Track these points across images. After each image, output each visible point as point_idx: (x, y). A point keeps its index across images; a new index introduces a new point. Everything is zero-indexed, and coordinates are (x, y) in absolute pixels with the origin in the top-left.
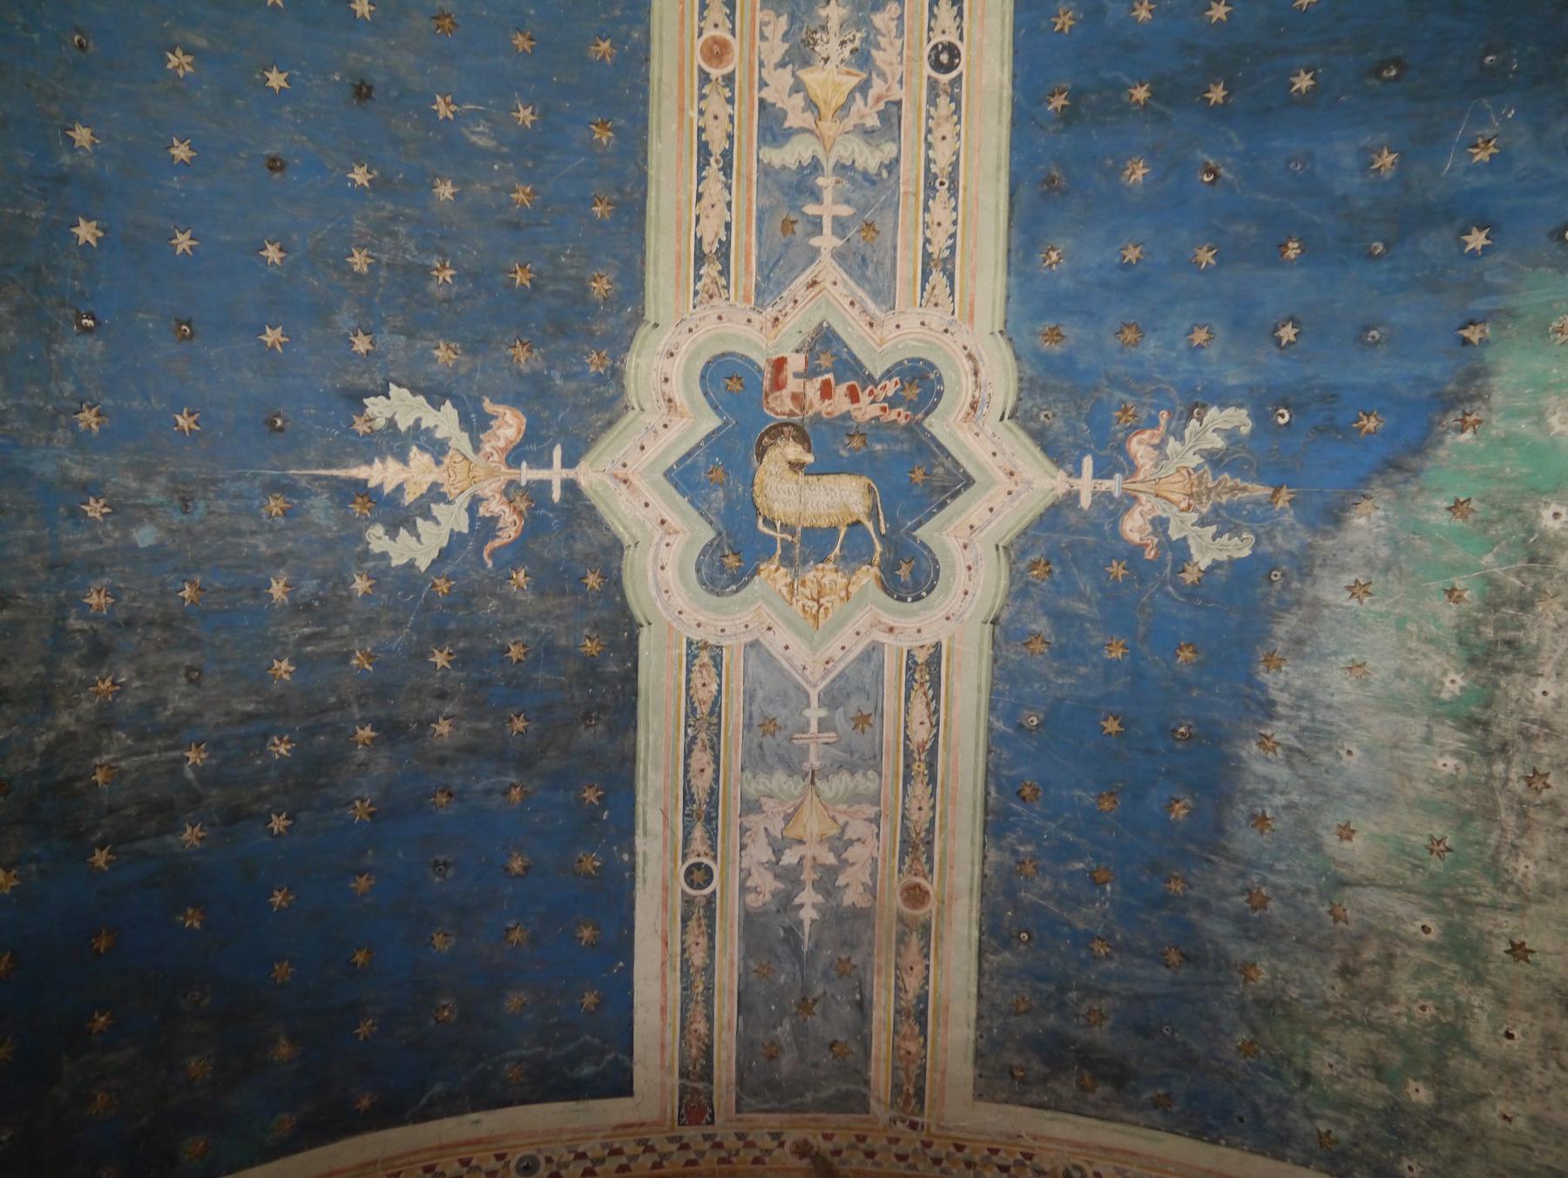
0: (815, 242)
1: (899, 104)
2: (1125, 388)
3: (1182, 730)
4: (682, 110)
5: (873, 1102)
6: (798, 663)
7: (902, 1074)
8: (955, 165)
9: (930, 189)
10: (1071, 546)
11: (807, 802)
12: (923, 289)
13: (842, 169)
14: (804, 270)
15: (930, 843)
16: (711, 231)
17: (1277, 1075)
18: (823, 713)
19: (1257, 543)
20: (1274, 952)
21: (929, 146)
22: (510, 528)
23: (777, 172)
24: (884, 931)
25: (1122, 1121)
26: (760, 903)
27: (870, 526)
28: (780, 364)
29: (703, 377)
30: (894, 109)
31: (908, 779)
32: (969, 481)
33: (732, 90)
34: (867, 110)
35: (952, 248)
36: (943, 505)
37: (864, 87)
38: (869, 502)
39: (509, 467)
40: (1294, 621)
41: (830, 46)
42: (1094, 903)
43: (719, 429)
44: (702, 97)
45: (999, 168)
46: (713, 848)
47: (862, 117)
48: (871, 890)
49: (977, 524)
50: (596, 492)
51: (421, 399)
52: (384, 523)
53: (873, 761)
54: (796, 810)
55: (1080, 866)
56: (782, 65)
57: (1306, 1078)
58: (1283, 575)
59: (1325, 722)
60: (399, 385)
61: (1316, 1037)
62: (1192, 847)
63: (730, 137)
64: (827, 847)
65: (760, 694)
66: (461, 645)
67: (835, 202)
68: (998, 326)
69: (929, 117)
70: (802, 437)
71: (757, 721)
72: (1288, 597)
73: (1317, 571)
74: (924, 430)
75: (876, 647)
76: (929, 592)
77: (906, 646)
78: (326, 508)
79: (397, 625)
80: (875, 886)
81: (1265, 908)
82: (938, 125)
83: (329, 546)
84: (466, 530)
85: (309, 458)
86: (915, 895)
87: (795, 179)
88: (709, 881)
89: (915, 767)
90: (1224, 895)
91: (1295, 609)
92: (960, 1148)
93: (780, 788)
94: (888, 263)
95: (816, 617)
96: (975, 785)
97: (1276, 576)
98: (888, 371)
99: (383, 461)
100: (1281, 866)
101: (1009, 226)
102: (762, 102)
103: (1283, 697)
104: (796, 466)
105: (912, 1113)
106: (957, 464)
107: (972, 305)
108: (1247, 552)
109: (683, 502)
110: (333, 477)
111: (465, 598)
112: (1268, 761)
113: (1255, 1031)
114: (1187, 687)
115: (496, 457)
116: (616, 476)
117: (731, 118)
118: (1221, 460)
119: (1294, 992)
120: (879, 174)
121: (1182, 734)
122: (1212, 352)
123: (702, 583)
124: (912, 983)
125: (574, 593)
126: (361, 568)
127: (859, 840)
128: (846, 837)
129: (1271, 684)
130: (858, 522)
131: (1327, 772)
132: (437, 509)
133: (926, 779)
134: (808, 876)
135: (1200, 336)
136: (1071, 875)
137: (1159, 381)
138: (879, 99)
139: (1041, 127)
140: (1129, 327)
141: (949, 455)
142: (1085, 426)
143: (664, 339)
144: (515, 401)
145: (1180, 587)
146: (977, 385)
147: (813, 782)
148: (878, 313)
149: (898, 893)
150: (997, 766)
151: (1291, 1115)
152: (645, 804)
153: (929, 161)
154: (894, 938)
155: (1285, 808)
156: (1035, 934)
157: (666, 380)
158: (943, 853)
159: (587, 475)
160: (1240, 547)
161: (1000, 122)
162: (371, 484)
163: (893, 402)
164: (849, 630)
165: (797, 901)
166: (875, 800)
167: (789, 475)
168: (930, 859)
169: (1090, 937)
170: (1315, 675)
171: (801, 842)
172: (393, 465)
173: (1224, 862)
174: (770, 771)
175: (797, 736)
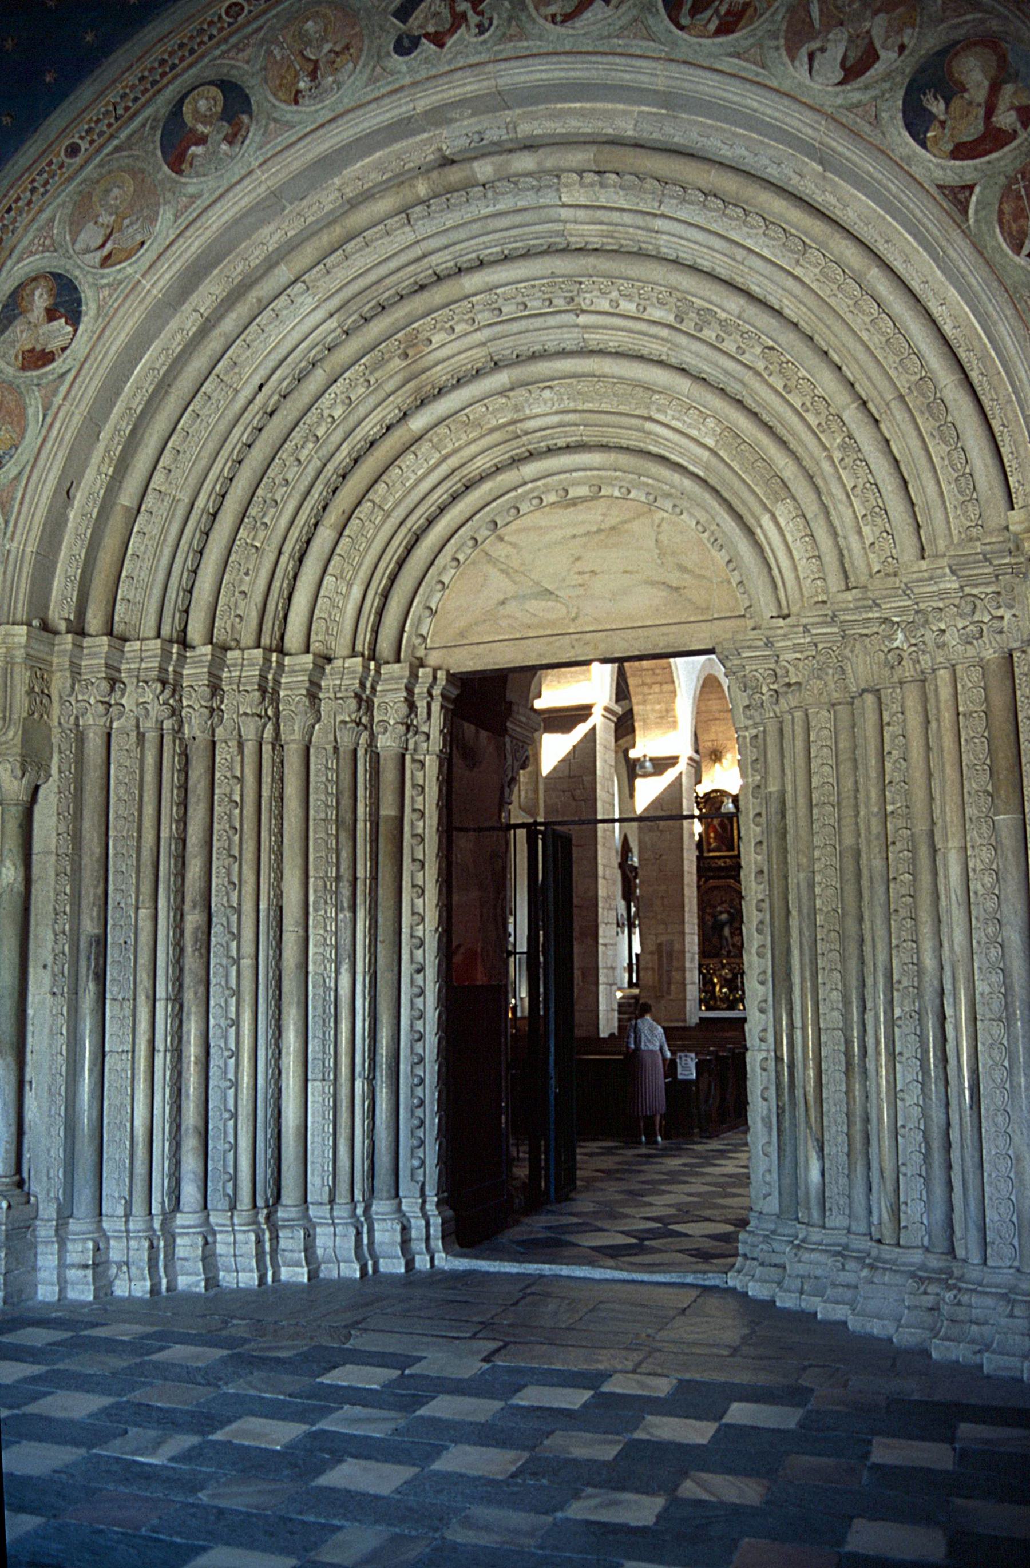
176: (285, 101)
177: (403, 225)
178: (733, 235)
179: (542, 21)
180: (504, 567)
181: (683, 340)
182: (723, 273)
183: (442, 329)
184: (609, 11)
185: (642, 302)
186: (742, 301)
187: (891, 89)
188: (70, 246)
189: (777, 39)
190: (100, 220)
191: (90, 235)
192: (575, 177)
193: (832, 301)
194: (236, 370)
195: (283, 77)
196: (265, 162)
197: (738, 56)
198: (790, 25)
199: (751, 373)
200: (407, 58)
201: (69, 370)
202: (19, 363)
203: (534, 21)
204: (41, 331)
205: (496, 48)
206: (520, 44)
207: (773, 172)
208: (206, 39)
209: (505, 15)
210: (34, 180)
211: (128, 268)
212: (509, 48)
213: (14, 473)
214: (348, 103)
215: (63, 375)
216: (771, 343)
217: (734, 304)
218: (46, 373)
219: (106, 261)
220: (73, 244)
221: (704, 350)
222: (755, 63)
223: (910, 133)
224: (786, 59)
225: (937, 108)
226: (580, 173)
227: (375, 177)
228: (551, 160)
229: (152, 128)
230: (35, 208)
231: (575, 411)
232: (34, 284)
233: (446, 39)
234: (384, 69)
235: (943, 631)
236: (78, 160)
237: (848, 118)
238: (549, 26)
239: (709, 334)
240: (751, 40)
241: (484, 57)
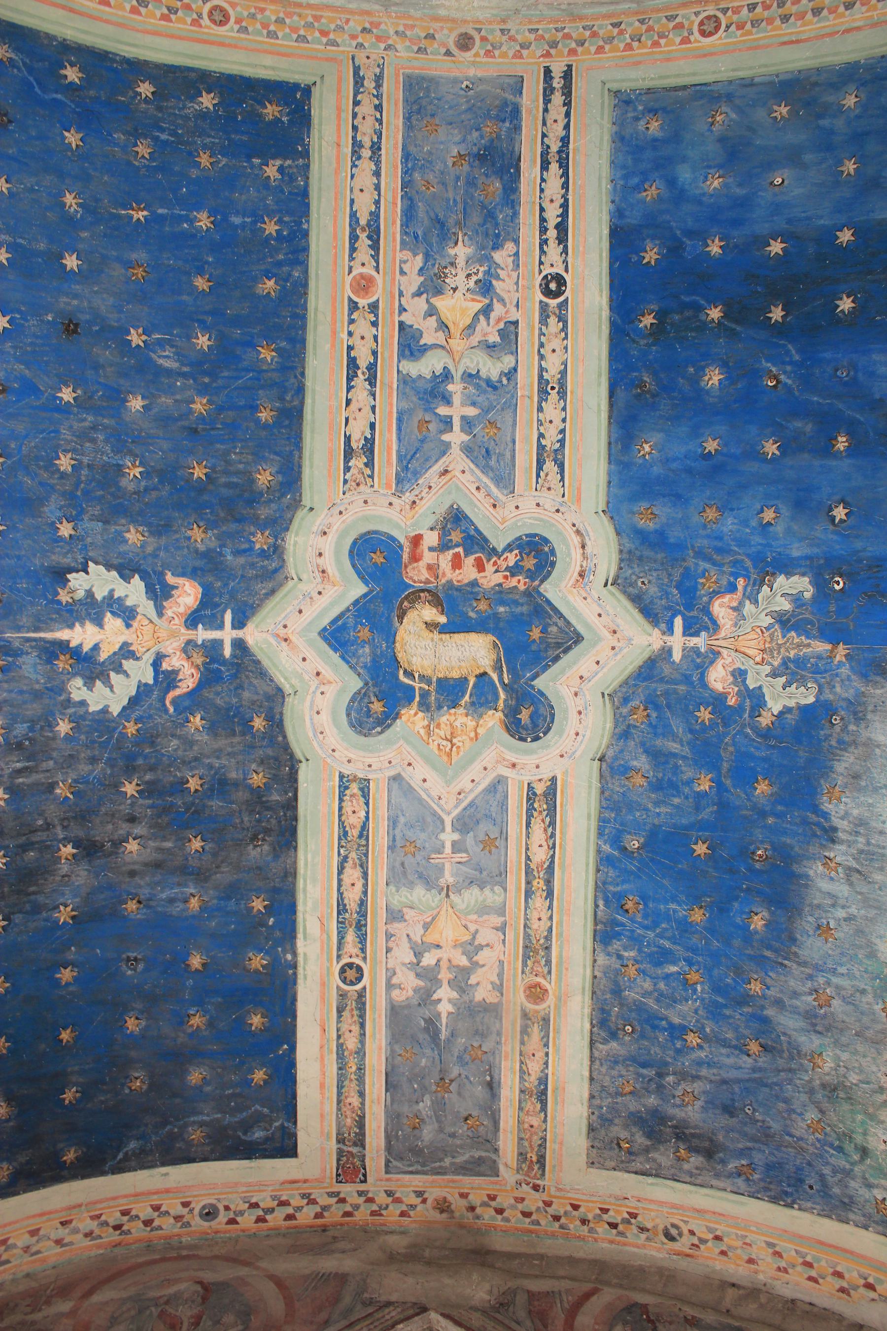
0: (446, 437)
1: (516, 323)
2: (708, 559)
3: (760, 852)
4: (334, 333)
5: (502, 1168)
6: (435, 794)
7: (526, 1144)
8: (563, 373)
9: (543, 393)
10: (666, 693)
11: (443, 912)
12: (538, 476)
13: (470, 377)
14: (436, 461)
15: (548, 948)
16: (358, 431)
17: (840, 1149)
18: (456, 836)
19: (820, 691)
20: (836, 1043)
21: (542, 357)
22: (189, 679)
23: (414, 381)
24: (511, 1023)
25: (712, 1187)
26: (404, 998)
27: (495, 677)
28: (416, 540)
29: (351, 552)
30: (512, 328)
31: (529, 894)
32: (578, 638)
33: (377, 316)
34: (489, 329)
35: (562, 442)
36: (556, 659)
37: (486, 311)
38: (494, 657)
39: (187, 628)
40: (852, 759)
41: (458, 278)
42: (687, 1001)
43: (365, 596)
44: (352, 322)
45: (600, 375)
46: (363, 950)
47: (485, 335)
48: (499, 988)
49: (585, 676)
50: (261, 649)
51: (114, 573)
52: (83, 677)
53: (500, 877)
54: (433, 919)
55: (674, 969)
56: (418, 294)
57: (864, 1152)
58: (842, 719)
59: (878, 846)
60: (96, 563)
61: (872, 1117)
62: (768, 953)
63: (375, 353)
64: (460, 950)
65: (402, 820)
66: (148, 777)
67: (463, 405)
68: (602, 506)
69: (542, 334)
70: (436, 601)
71: (399, 843)
72: (846, 739)
73: (869, 716)
74: (540, 595)
75: (500, 782)
76: (545, 734)
77: (526, 779)
78: (35, 665)
79: (93, 760)
80: (502, 985)
81: (830, 1006)
82: (549, 341)
83: (37, 695)
84: (151, 682)
85: (21, 624)
86: (536, 993)
87: (429, 386)
88: (359, 979)
89: (535, 883)
90: (795, 994)
91: (851, 749)
92: (576, 1207)
93: (420, 900)
94: (508, 455)
95: (449, 755)
96: (586, 899)
97: (836, 719)
98: (509, 545)
99: (82, 625)
100: (842, 970)
101: (610, 423)
102: (401, 324)
103: (842, 824)
104: (431, 626)
105: (535, 1177)
106: (568, 623)
107: (579, 489)
108: (811, 700)
109: (335, 657)
110: (41, 639)
111: (149, 738)
112: (832, 879)
113: (822, 1112)
114: (763, 814)
115: (177, 621)
116: (278, 636)
117: (376, 338)
118: (788, 620)
119: (854, 1078)
120: (500, 381)
121: (761, 857)
122: (779, 529)
123: (352, 725)
124: (534, 1067)
125: (243, 734)
126: (64, 714)
127: (487, 945)
128: (476, 943)
129: (833, 813)
130: (485, 674)
131: (880, 889)
132: (127, 664)
133: (545, 894)
134: (445, 975)
135: (769, 515)
136: (667, 977)
137: (736, 553)
138: (499, 320)
139: (634, 341)
140: (710, 507)
141: (561, 616)
142: (675, 591)
143: (319, 520)
144: (193, 573)
145: (755, 729)
146: (585, 557)
147: (448, 896)
148: (500, 496)
149: (522, 990)
150: (604, 883)
151: (852, 1184)
152: (305, 912)
153: (542, 369)
154: (518, 1029)
155: (845, 920)
156: (638, 1028)
157: (320, 554)
158: (560, 957)
159: (252, 634)
160: (805, 695)
161: (600, 337)
162: (73, 644)
163: (514, 571)
164: (477, 766)
165: (435, 997)
166: (501, 911)
167: (426, 633)
168: (548, 962)
169: (683, 1030)
170: (870, 805)
171: (438, 946)
172: (90, 628)
173: (795, 966)
174: (411, 885)
175: (433, 856)
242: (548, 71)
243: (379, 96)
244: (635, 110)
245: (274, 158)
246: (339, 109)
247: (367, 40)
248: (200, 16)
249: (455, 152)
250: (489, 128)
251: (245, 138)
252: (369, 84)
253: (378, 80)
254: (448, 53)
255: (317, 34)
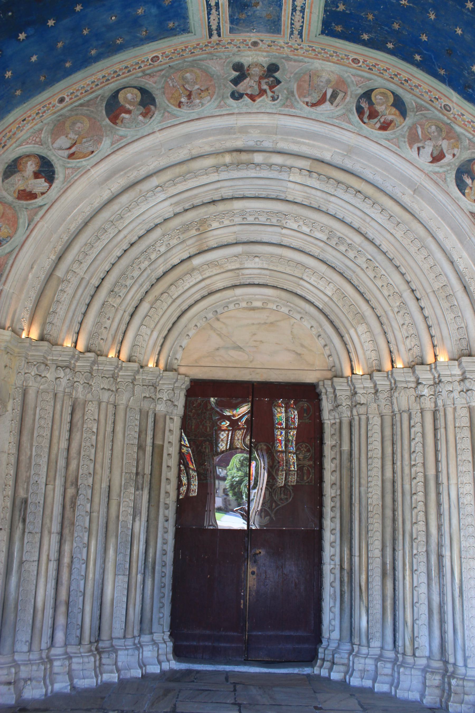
176: (174, 105)
177: (215, 172)
178: (365, 210)
179: (302, 103)
180: (219, 333)
181: (329, 249)
182: (356, 225)
183: (218, 221)
184: (332, 107)
185: (313, 229)
186: (362, 238)
187: (450, 170)
188: (50, 144)
189: (404, 138)
190: (69, 136)
191: (63, 142)
192: (298, 170)
193: (407, 247)
194: (122, 221)
195: (173, 94)
196: (162, 129)
197: (389, 141)
198: (409, 134)
199: (359, 269)
200: (237, 101)
201: (45, 205)
202: (16, 195)
203: (298, 102)
204: (30, 182)
205: (280, 109)
206: (291, 110)
207: (389, 189)
208: (137, 67)
209: (285, 96)
210: (40, 109)
211: (84, 162)
212: (286, 110)
213: (8, 250)
214: (206, 113)
215: (41, 207)
216: (370, 257)
217: (358, 239)
218: (32, 204)
219: (71, 156)
220: (52, 144)
221: (339, 256)
222: (396, 145)
223: (459, 189)
224: (408, 147)
225: (469, 181)
226: (301, 170)
227: (208, 149)
228: (290, 161)
229: (101, 100)
230: (35, 122)
231: (267, 269)
232: (27, 159)
233: (256, 98)
234: (225, 103)
235: (452, 391)
236: (61, 105)
237: (434, 177)
238: (305, 106)
239: (342, 248)
240: (394, 136)
241: (274, 111)
242: (219, 35)
243: (292, 28)
244: (180, 28)
245: (340, 12)
246: (309, 25)
247: (296, 46)
248: (363, 62)
249: (258, 8)
250: (243, 16)
251: (351, 21)
252: (296, 32)
253: (292, 33)
254: (262, 41)
255: (317, 50)
